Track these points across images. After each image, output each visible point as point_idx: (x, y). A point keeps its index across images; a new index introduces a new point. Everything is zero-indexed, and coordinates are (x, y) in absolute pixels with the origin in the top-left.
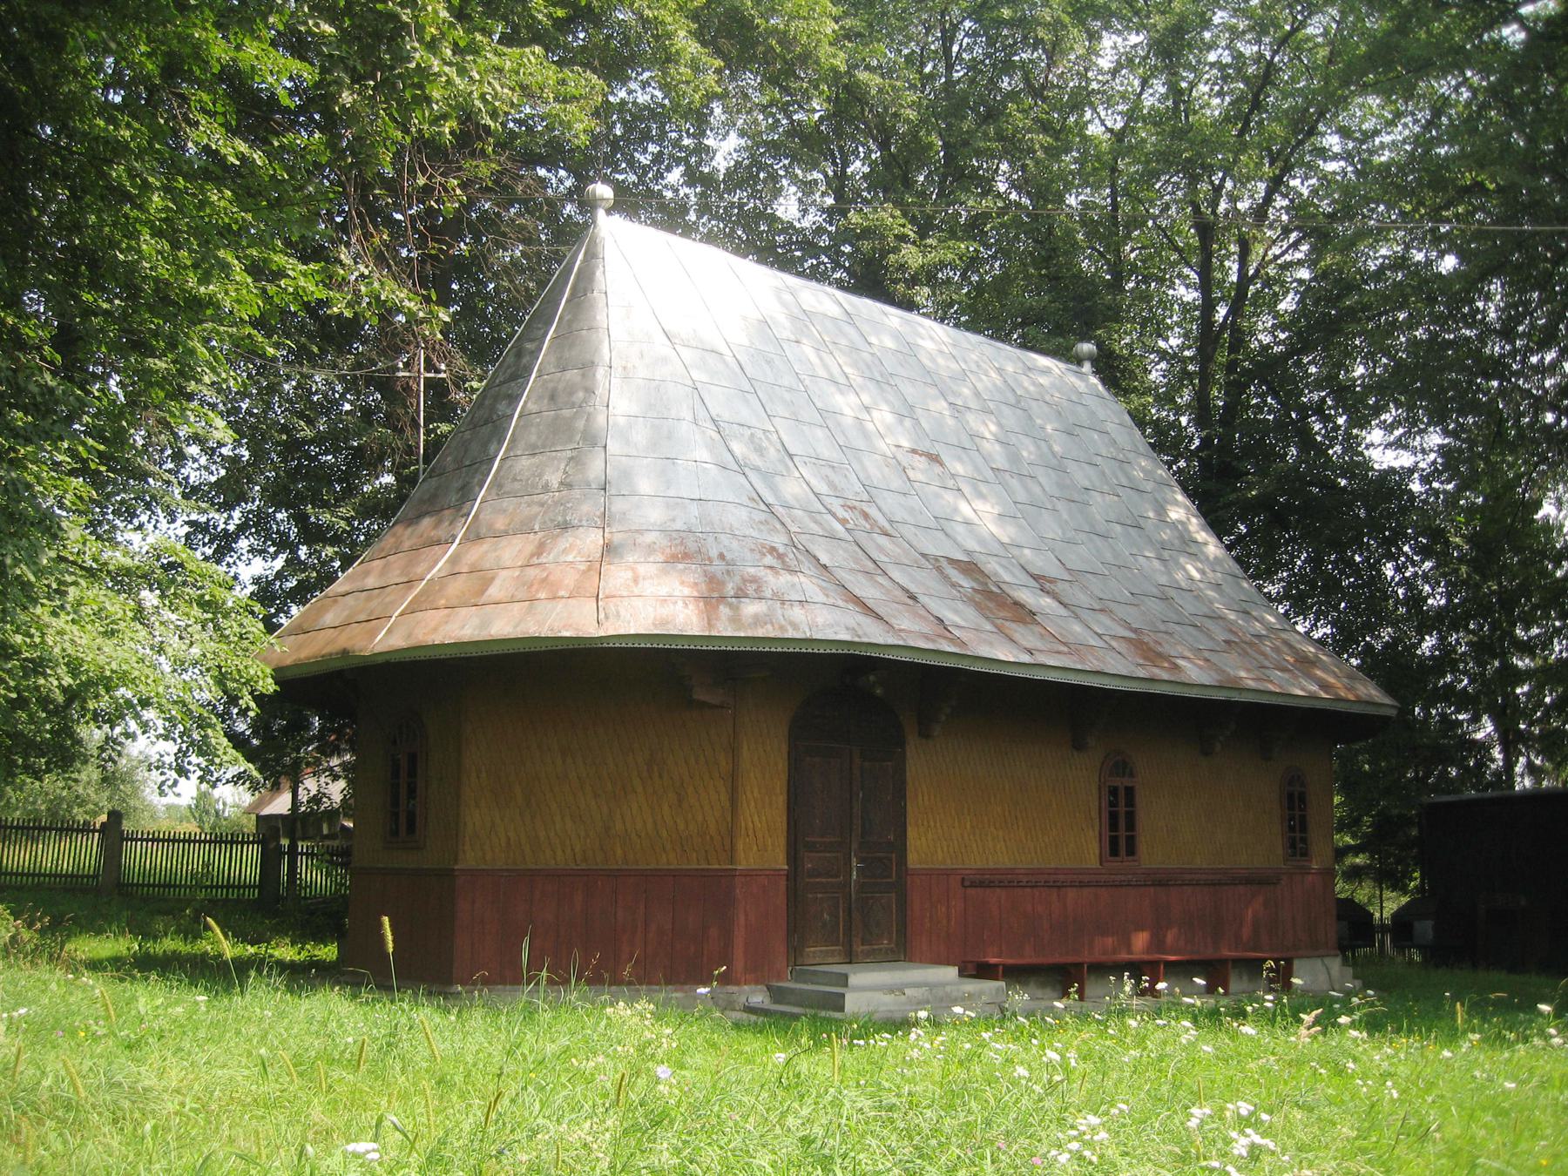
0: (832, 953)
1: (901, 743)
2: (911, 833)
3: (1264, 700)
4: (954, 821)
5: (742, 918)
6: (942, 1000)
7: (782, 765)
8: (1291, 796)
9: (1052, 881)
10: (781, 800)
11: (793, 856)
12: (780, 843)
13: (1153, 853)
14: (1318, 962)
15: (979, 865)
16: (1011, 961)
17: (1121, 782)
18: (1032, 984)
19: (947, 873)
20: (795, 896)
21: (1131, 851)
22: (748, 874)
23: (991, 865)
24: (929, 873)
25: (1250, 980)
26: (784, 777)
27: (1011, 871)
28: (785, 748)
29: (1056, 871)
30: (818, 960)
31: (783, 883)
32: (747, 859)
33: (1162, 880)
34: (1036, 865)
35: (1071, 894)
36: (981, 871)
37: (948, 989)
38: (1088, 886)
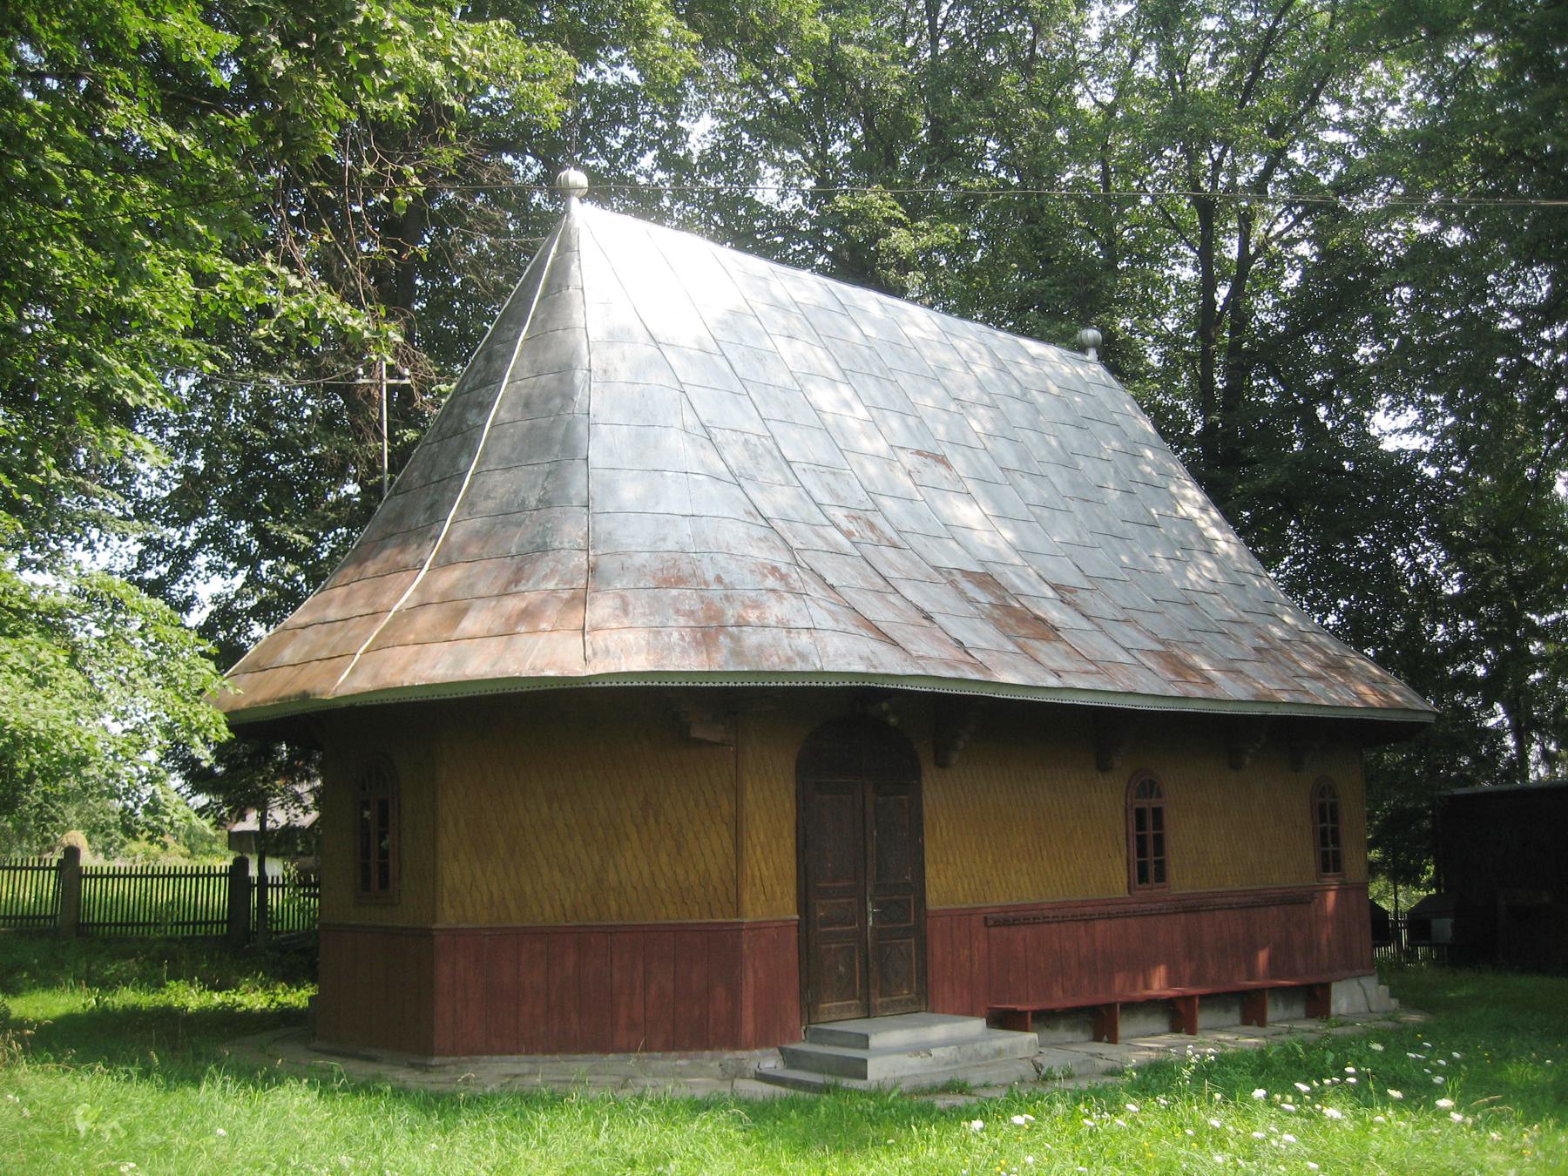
1: (917, 773)
2: (930, 871)
3: (1311, 713)
4: (978, 856)
7: (789, 807)
8: (1322, 809)
10: (789, 843)
11: (804, 905)
13: (1183, 879)
14: (1354, 983)
15: (1002, 901)
16: (1035, 1007)
17: (1148, 803)
18: (1061, 1028)
21: (1161, 876)
22: (756, 927)
23: (1015, 901)
24: (950, 914)
25: (1286, 1008)
27: (1035, 907)
28: (792, 787)
29: (1084, 903)
30: (834, 1017)
31: (794, 934)
32: (754, 910)
33: (1192, 907)
34: (1061, 899)
35: (1100, 926)
36: (1005, 909)
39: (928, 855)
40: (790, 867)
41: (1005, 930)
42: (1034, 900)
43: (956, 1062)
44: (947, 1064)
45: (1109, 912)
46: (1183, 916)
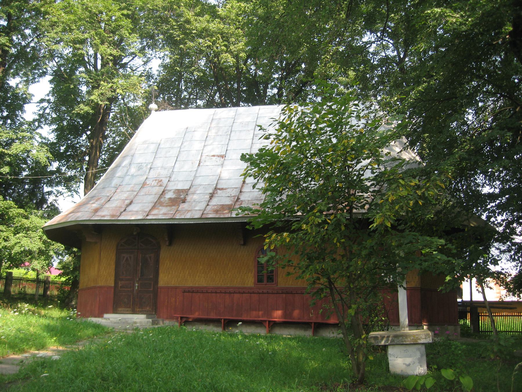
0: (128, 310)
1: (159, 248)
5: (98, 299)
6: (124, 323)
7: (114, 257)
9: (242, 291)
10: (113, 267)
11: (116, 283)
12: (113, 278)
15: (191, 285)
19: (176, 288)
20: (115, 294)
22: (101, 287)
23: (197, 285)
24: (168, 288)
26: (115, 260)
31: (113, 290)
32: (101, 283)
34: (219, 285)
35: (236, 296)
36: (192, 288)
37: (127, 320)
38: (244, 293)
39: (160, 271)
40: (113, 273)
41: (191, 294)
42: (205, 285)
43: (118, 323)
44: (115, 323)
45: (249, 291)
46: (284, 295)
